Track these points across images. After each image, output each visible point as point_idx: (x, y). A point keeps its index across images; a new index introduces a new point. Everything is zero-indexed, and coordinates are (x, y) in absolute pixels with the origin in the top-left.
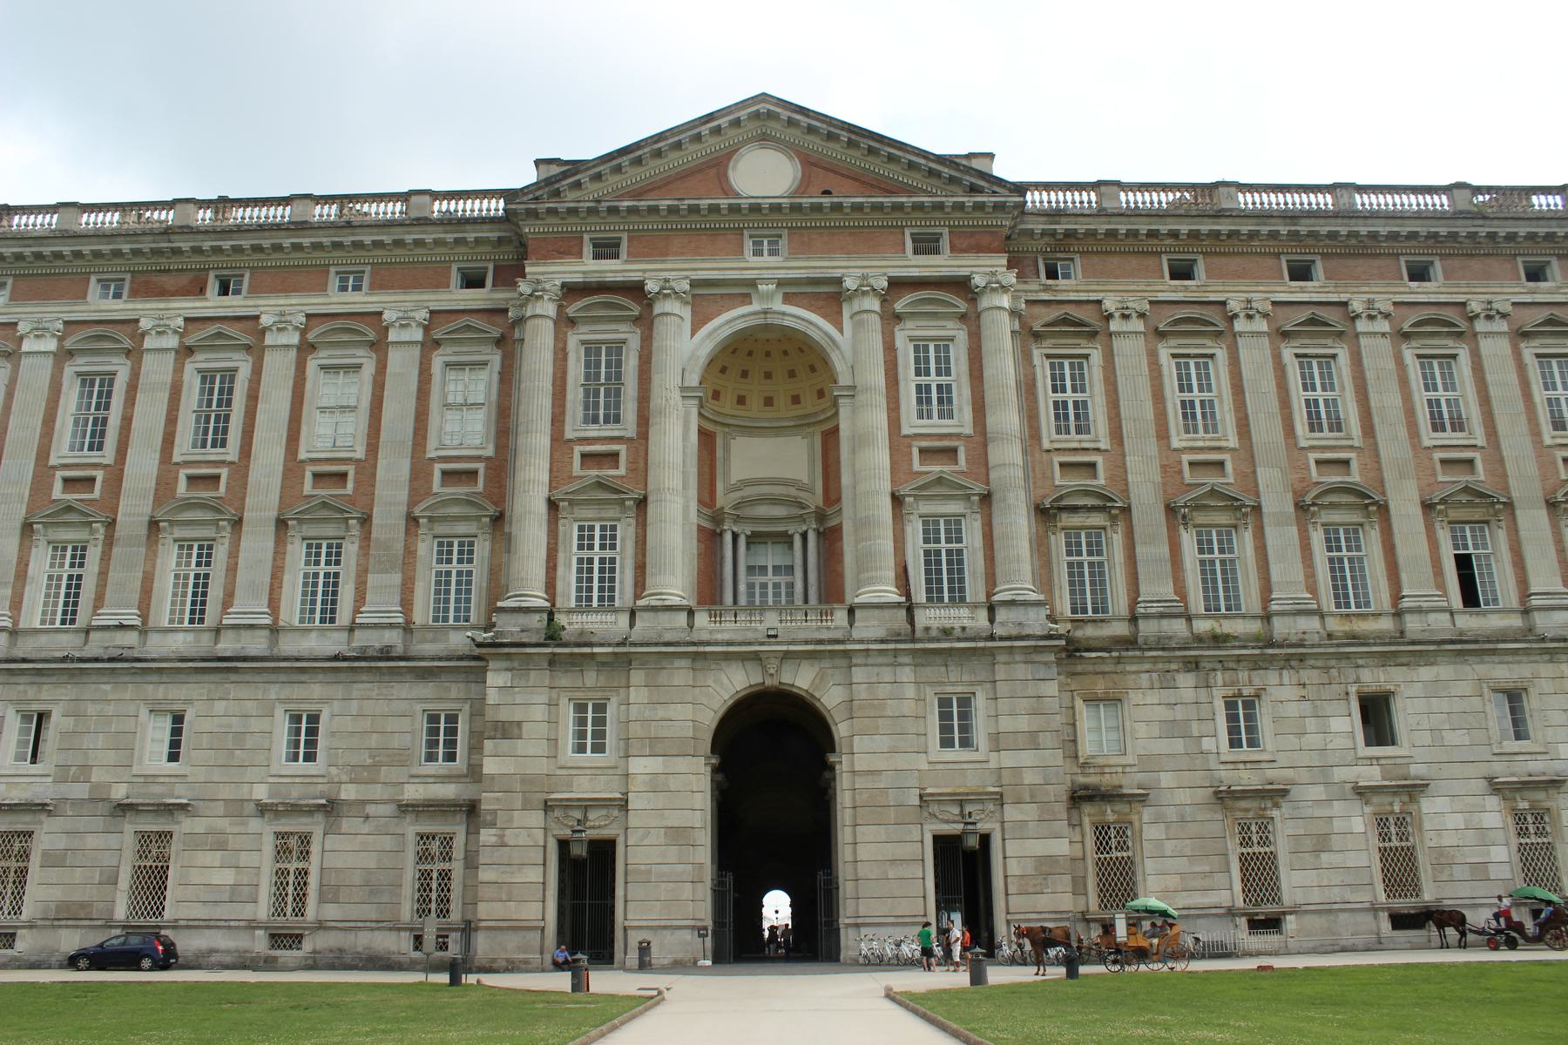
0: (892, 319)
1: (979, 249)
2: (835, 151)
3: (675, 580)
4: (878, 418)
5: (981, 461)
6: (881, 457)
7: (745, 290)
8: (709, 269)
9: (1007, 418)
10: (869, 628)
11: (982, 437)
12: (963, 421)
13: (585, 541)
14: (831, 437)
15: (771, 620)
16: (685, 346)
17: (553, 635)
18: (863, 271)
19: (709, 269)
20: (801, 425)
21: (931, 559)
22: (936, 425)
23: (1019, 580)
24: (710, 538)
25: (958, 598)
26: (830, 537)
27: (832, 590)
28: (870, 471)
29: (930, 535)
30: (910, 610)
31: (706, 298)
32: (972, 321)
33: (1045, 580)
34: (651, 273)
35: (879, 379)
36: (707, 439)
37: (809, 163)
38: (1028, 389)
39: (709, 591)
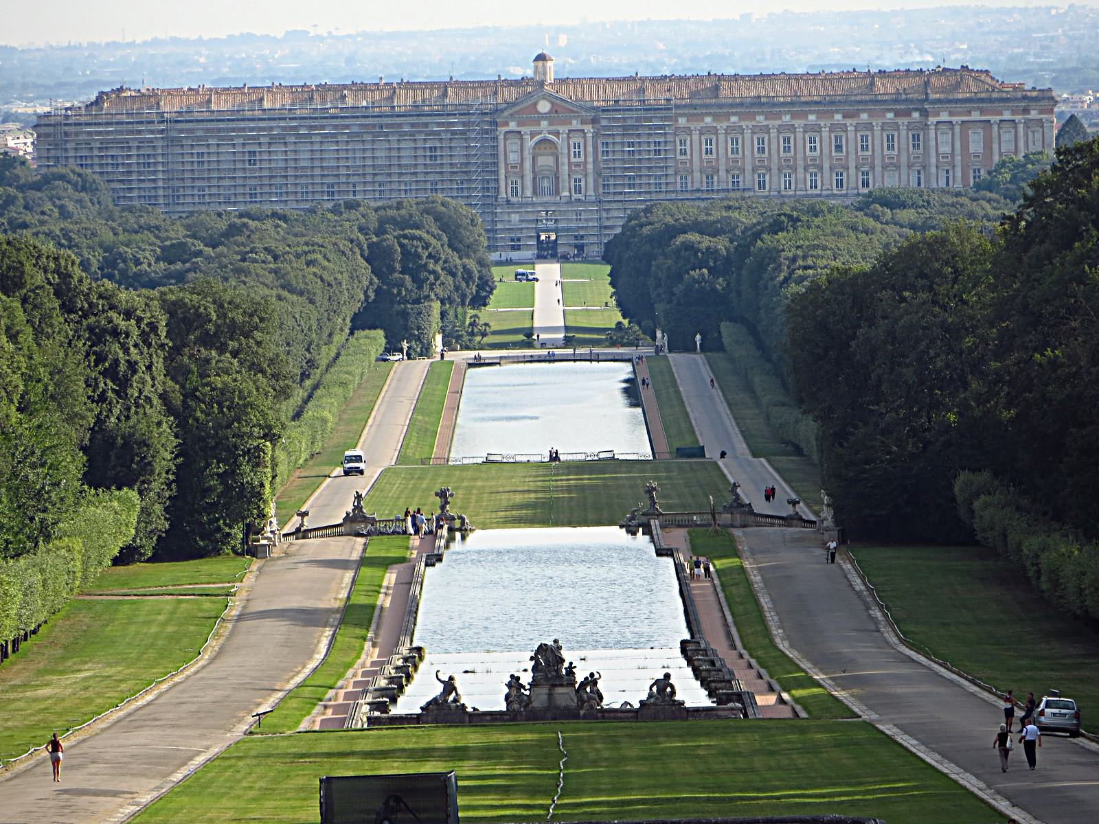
0: (569, 138)
1: (587, 123)
2: (558, 102)
3: (529, 193)
4: (566, 160)
5: (585, 167)
6: (566, 168)
7: (540, 133)
8: (534, 129)
9: (590, 159)
10: (563, 200)
11: (585, 162)
12: (582, 159)
13: (512, 183)
14: (557, 158)
15: (546, 199)
16: (530, 143)
17: (508, 201)
18: (563, 129)
19: (534, 129)
20: (552, 154)
21: (575, 186)
22: (577, 160)
23: (591, 192)
24: (534, 179)
25: (580, 193)
26: (557, 178)
27: (557, 193)
28: (565, 169)
29: (575, 181)
30: (571, 196)
31: (533, 135)
32: (585, 138)
33: (596, 189)
34: (523, 129)
35: (566, 151)
36: (533, 158)
37: (553, 104)
38: (595, 148)
39: (535, 192)
